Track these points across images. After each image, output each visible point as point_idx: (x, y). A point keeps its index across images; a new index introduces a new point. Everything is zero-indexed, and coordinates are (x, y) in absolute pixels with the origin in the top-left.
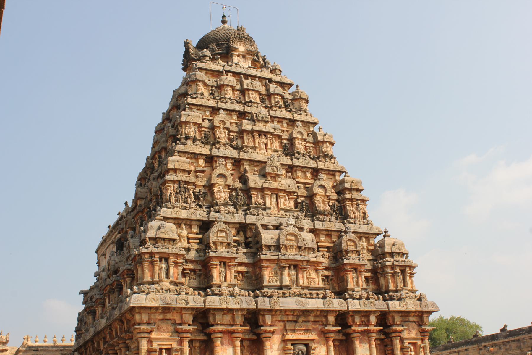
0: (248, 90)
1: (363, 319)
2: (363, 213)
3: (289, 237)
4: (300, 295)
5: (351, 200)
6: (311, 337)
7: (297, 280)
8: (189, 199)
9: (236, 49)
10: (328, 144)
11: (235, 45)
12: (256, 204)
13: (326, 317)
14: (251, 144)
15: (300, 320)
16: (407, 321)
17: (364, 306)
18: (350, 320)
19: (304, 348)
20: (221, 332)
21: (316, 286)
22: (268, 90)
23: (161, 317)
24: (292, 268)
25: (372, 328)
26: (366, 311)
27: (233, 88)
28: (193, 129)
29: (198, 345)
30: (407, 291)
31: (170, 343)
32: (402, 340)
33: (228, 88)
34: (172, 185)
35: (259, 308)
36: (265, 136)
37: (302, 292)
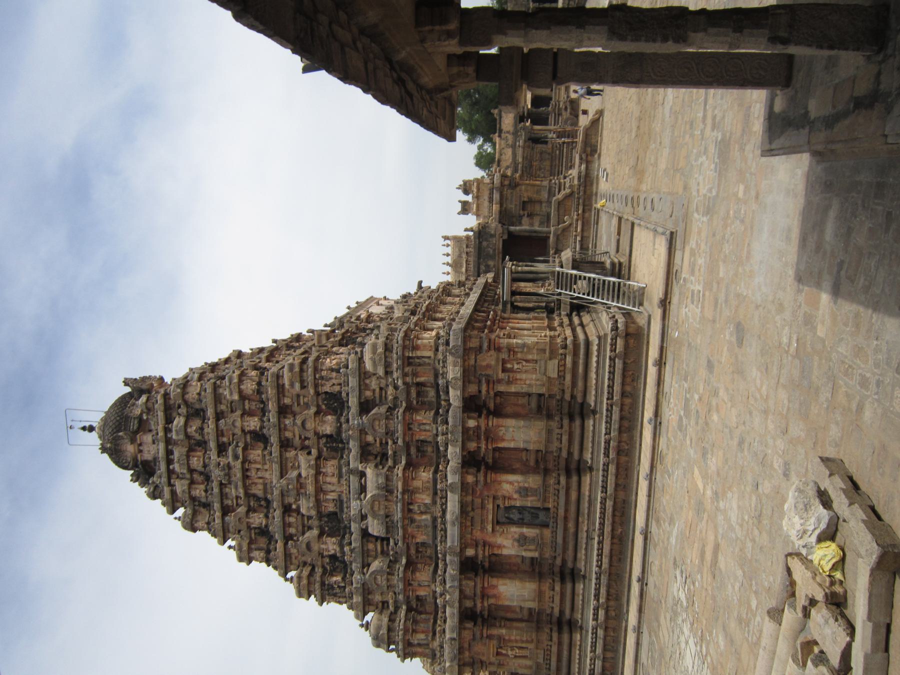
3: (376, 508)
4: (444, 512)
5: (316, 386)
6: (490, 506)
10: (242, 387)
14: (261, 487)
16: (475, 367)
26: (463, 433)
32: (499, 381)
36: (247, 470)
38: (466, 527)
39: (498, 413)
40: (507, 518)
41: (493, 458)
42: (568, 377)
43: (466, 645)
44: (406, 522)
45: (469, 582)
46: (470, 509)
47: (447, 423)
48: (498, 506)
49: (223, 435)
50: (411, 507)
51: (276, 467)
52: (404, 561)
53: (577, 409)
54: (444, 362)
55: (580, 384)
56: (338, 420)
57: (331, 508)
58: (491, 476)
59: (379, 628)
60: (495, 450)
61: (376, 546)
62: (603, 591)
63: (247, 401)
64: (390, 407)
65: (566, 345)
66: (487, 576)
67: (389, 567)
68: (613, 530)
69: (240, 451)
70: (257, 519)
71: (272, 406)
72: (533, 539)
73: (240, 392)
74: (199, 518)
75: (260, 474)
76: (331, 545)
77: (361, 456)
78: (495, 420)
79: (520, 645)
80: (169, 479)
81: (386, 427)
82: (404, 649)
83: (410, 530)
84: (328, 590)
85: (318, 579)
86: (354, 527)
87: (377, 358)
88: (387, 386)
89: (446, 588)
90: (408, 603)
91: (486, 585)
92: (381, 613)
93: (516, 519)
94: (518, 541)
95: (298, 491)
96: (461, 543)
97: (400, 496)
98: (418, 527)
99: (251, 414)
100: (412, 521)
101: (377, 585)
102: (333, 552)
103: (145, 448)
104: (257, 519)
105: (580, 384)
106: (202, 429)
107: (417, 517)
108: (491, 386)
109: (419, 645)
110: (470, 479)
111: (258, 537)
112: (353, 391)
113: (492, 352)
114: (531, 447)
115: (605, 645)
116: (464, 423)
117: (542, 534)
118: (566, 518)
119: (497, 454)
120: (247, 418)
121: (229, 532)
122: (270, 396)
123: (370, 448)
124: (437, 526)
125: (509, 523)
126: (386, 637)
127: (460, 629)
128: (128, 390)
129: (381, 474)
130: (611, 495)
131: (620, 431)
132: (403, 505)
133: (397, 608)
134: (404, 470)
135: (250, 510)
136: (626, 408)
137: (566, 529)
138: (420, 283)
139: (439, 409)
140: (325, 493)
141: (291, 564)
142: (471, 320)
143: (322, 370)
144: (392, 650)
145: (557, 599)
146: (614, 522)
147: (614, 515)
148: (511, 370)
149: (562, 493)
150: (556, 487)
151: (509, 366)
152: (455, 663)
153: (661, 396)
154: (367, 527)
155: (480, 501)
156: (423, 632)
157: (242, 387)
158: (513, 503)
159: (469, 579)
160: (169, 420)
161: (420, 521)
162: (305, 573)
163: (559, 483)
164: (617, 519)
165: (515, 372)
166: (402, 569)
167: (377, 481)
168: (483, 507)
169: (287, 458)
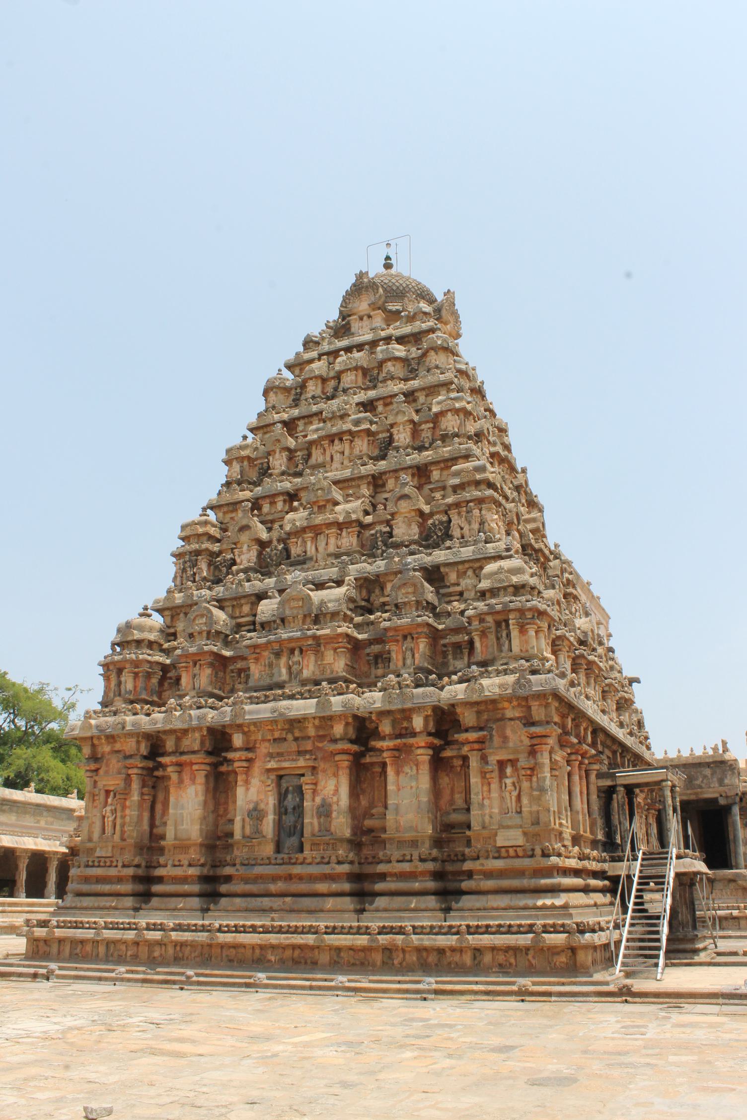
3: (294, 604)
4: (292, 697)
5: (457, 505)
6: (301, 763)
10: (449, 414)
16: (502, 719)
21: (334, 675)
26: (403, 711)
30: (505, 661)
32: (484, 759)
36: (341, 440)
39: (438, 764)
40: (287, 791)
41: (372, 764)
42: (499, 864)
43: (118, 746)
44: (276, 647)
45: (198, 742)
46: (297, 734)
47: (417, 686)
48: (303, 775)
49: (386, 405)
50: (297, 652)
51: (347, 473)
52: (227, 653)
53: (452, 886)
54: (506, 672)
55: (490, 884)
57: (295, 550)
58: (345, 762)
59: (141, 628)
60: (384, 765)
61: (247, 615)
62: (187, 936)
63: (431, 425)
64: (435, 608)
65: (549, 856)
66: (208, 768)
67: (218, 633)
68: (273, 947)
69: (364, 426)
70: (279, 462)
71: (427, 455)
73: (442, 413)
74: (281, 397)
75: (337, 457)
76: (247, 557)
77: (366, 579)
78: (427, 758)
79: (119, 821)
80: (328, 354)
81: (405, 603)
82: (114, 663)
83: (266, 654)
84: (190, 561)
85: (204, 546)
86: (271, 581)
87: (502, 576)
88: (466, 601)
89: (189, 713)
90: (173, 666)
91: (195, 767)
92: (161, 631)
93: (286, 803)
95: (315, 503)
96: (249, 725)
97: (309, 633)
98: (271, 665)
100: (278, 655)
101: (194, 619)
102: (238, 561)
104: (279, 462)
105: (490, 884)
106: (392, 378)
107: (283, 660)
108: (476, 746)
109: (119, 684)
111: (257, 468)
112: (454, 554)
113: (527, 742)
114: (390, 816)
115: (115, 942)
116: (418, 709)
118: (289, 878)
119: (378, 769)
120: (409, 427)
121: (265, 433)
122: (440, 451)
123: (377, 591)
124: (272, 688)
125: (280, 794)
126: (130, 638)
127: (138, 735)
128: (440, 297)
129: (340, 604)
130: (323, 941)
131: (420, 950)
132: (298, 639)
133: (167, 652)
134: (347, 635)
136: (457, 958)
137: (275, 878)
138: (637, 681)
139: (437, 669)
140: (315, 539)
141: (224, 513)
142: (580, 715)
144: (113, 649)
145: (178, 872)
146: (284, 948)
147: (294, 947)
148: (502, 775)
149: (326, 869)
150: (334, 859)
151: (509, 770)
152: (95, 732)
153: (468, 997)
154: (270, 598)
155: (309, 748)
156: (135, 687)
158: (308, 796)
159: (202, 743)
160: (401, 340)
161: (278, 666)
162: (212, 531)
163: (339, 863)
164: (289, 953)
165: (500, 782)
166: (215, 649)
167: (330, 601)
168: (300, 753)
169: (359, 486)
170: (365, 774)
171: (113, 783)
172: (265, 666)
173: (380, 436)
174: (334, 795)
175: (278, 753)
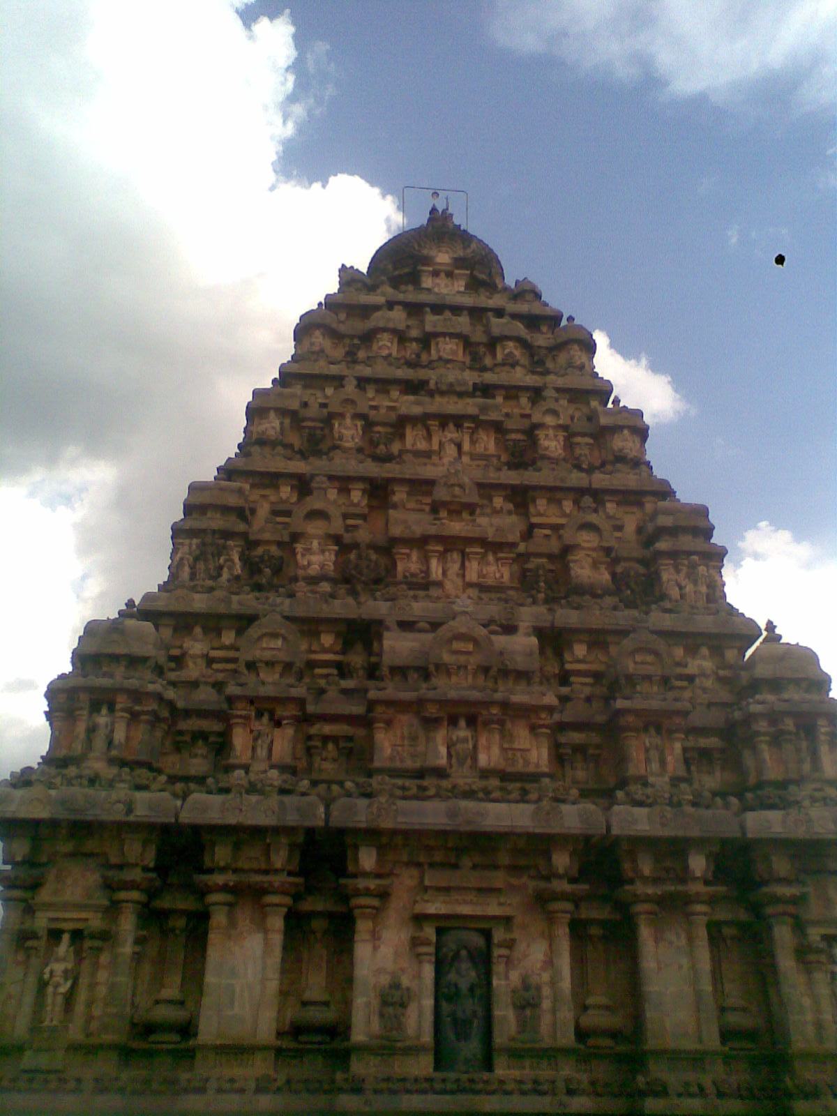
0: (436, 335)
1: (668, 864)
2: (708, 586)
3: (457, 645)
4: (469, 794)
5: (674, 555)
6: (493, 909)
7: (475, 759)
8: (225, 570)
9: (427, 261)
10: (626, 432)
11: (425, 252)
12: (405, 577)
13: (547, 855)
14: (422, 445)
15: (466, 862)
17: (663, 825)
18: (627, 866)
19: (479, 941)
20: (225, 888)
21: (531, 769)
22: (487, 331)
23: (68, 847)
24: (462, 723)
25: (697, 888)
26: (674, 841)
27: (401, 337)
28: (277, 423)
29: (181, 923)
30: (818, 785)
31: (84, 915)
33: (386, 336)
34: (187, 541)
35: (330, 824)
36: (459, 426)
37: (478, 784)
38: (429, 849)
40: (457, 956)
49: (506, 398)
50: (462, 723)
51: (478, 475)
56: (607, 592)
61: (325, 651)
70: (349, 433)
72: (400, 1027)
76: (317, 558)
93: (452, 977)
94: (396, 986)
95: (444, 504)
97: (498, 696)
98: (414, 738)
99: (569, 445)
100: (430, 723)
103: (442, 281)
104: (349, 433)
107: (440, 735)
110: (561, 861)
116: (700, 843)
117: (413, 1051)
127: (151, 827)
135: (369, 424)
140: (442, 556)
143: (707, 566)
155: (499, 884)
156: (128, 738)
157: (626, 432)
158: (499, 968)
160: (514, 316)
163: (570, 1092)
170: (609, 938)
171: (75, 915)
172: (403, 738)
173: (513, 436)
174: (543, 969)
175: (439, 889)
